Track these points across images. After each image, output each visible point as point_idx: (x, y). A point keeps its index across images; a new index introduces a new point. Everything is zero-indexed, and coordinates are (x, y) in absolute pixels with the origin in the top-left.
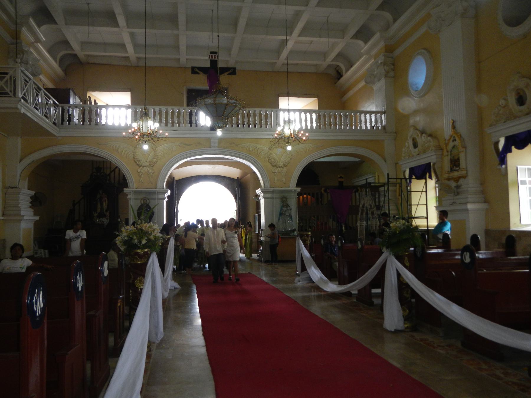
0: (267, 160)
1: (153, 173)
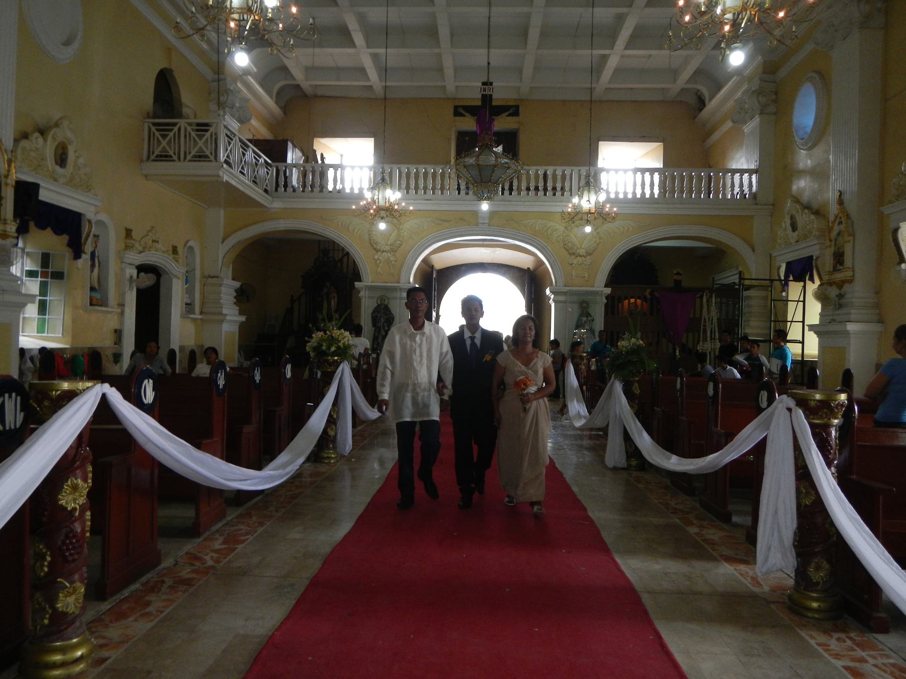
0: (562, 244)
1: (396, 261)
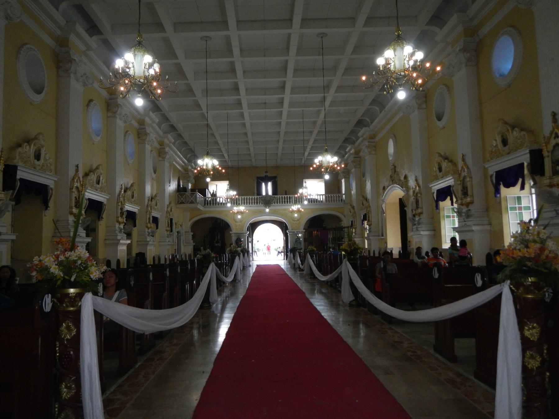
1: (242, 225)
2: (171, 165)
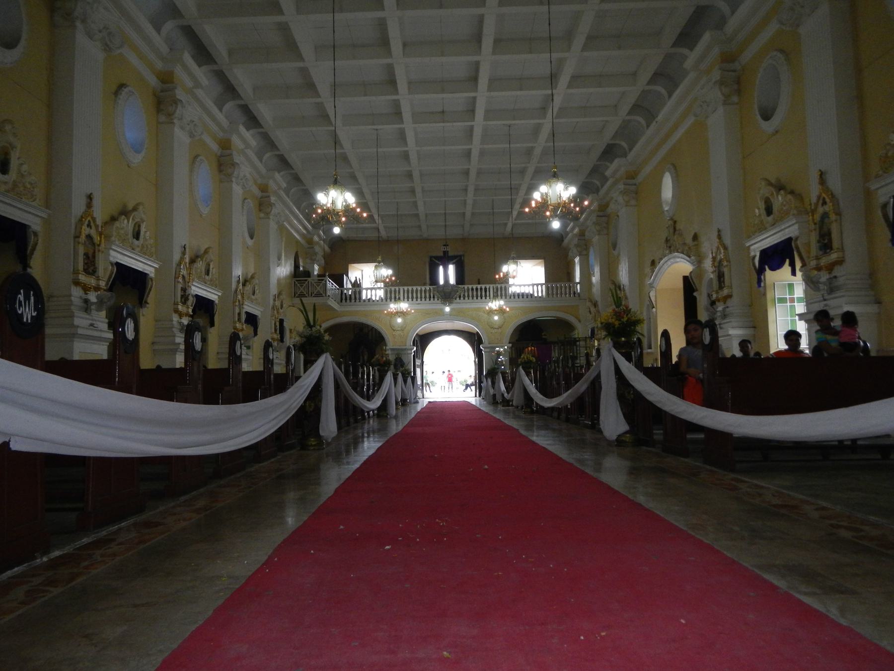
2: (281, 228)
